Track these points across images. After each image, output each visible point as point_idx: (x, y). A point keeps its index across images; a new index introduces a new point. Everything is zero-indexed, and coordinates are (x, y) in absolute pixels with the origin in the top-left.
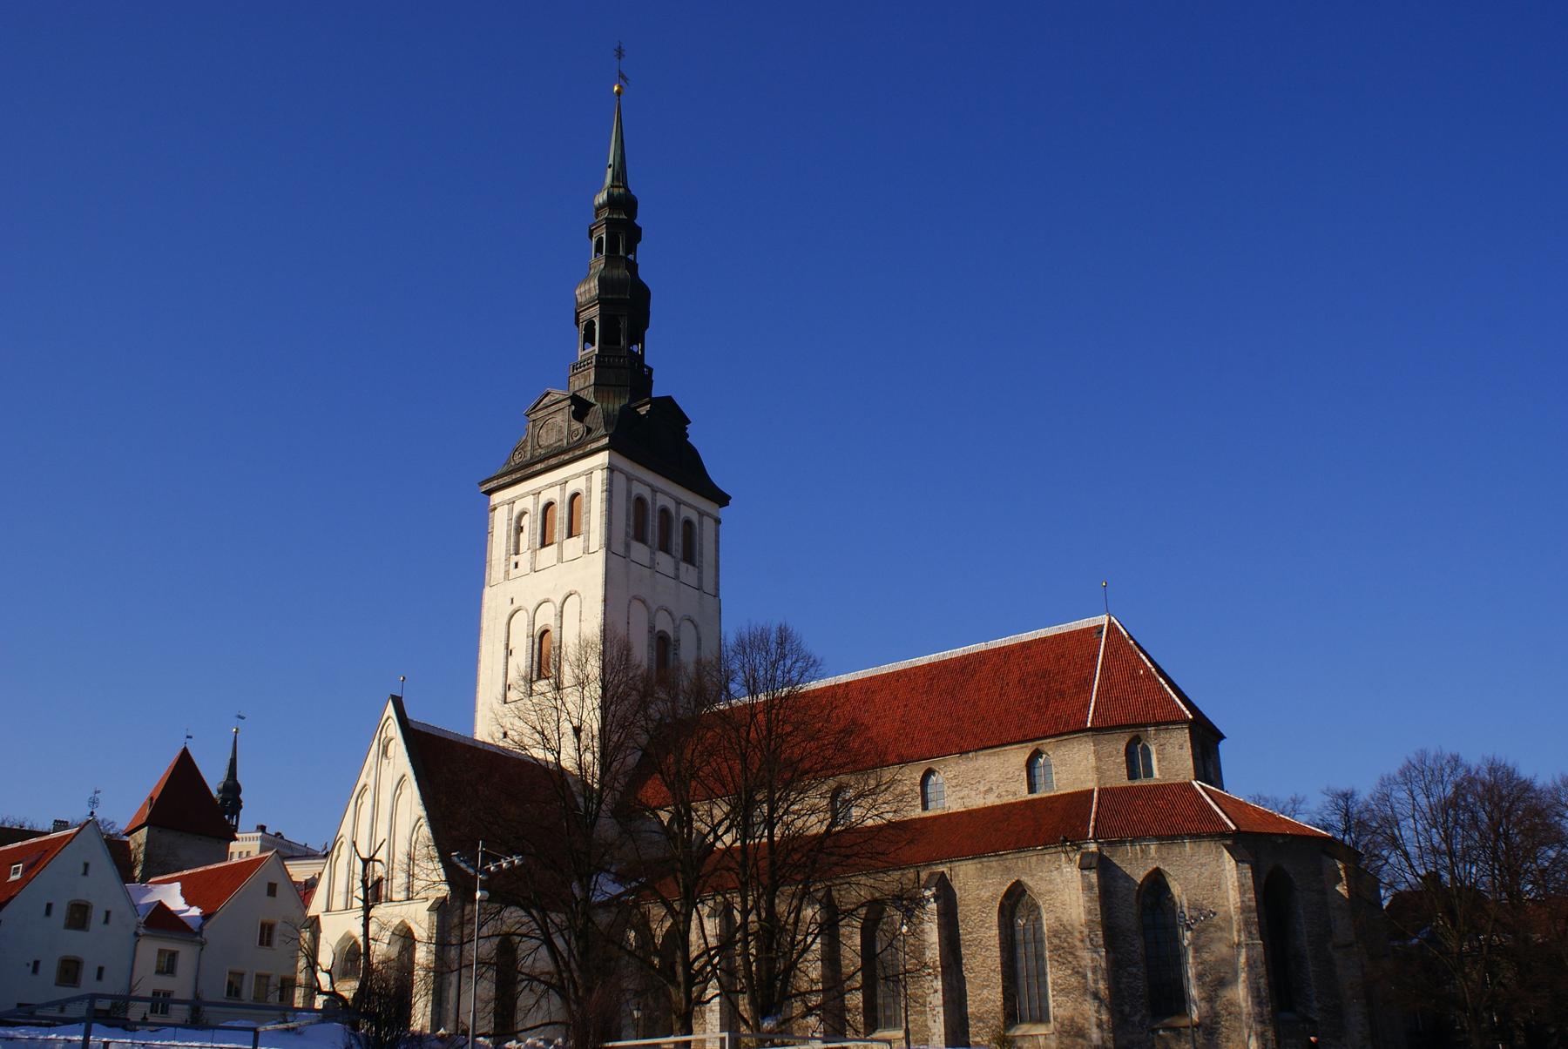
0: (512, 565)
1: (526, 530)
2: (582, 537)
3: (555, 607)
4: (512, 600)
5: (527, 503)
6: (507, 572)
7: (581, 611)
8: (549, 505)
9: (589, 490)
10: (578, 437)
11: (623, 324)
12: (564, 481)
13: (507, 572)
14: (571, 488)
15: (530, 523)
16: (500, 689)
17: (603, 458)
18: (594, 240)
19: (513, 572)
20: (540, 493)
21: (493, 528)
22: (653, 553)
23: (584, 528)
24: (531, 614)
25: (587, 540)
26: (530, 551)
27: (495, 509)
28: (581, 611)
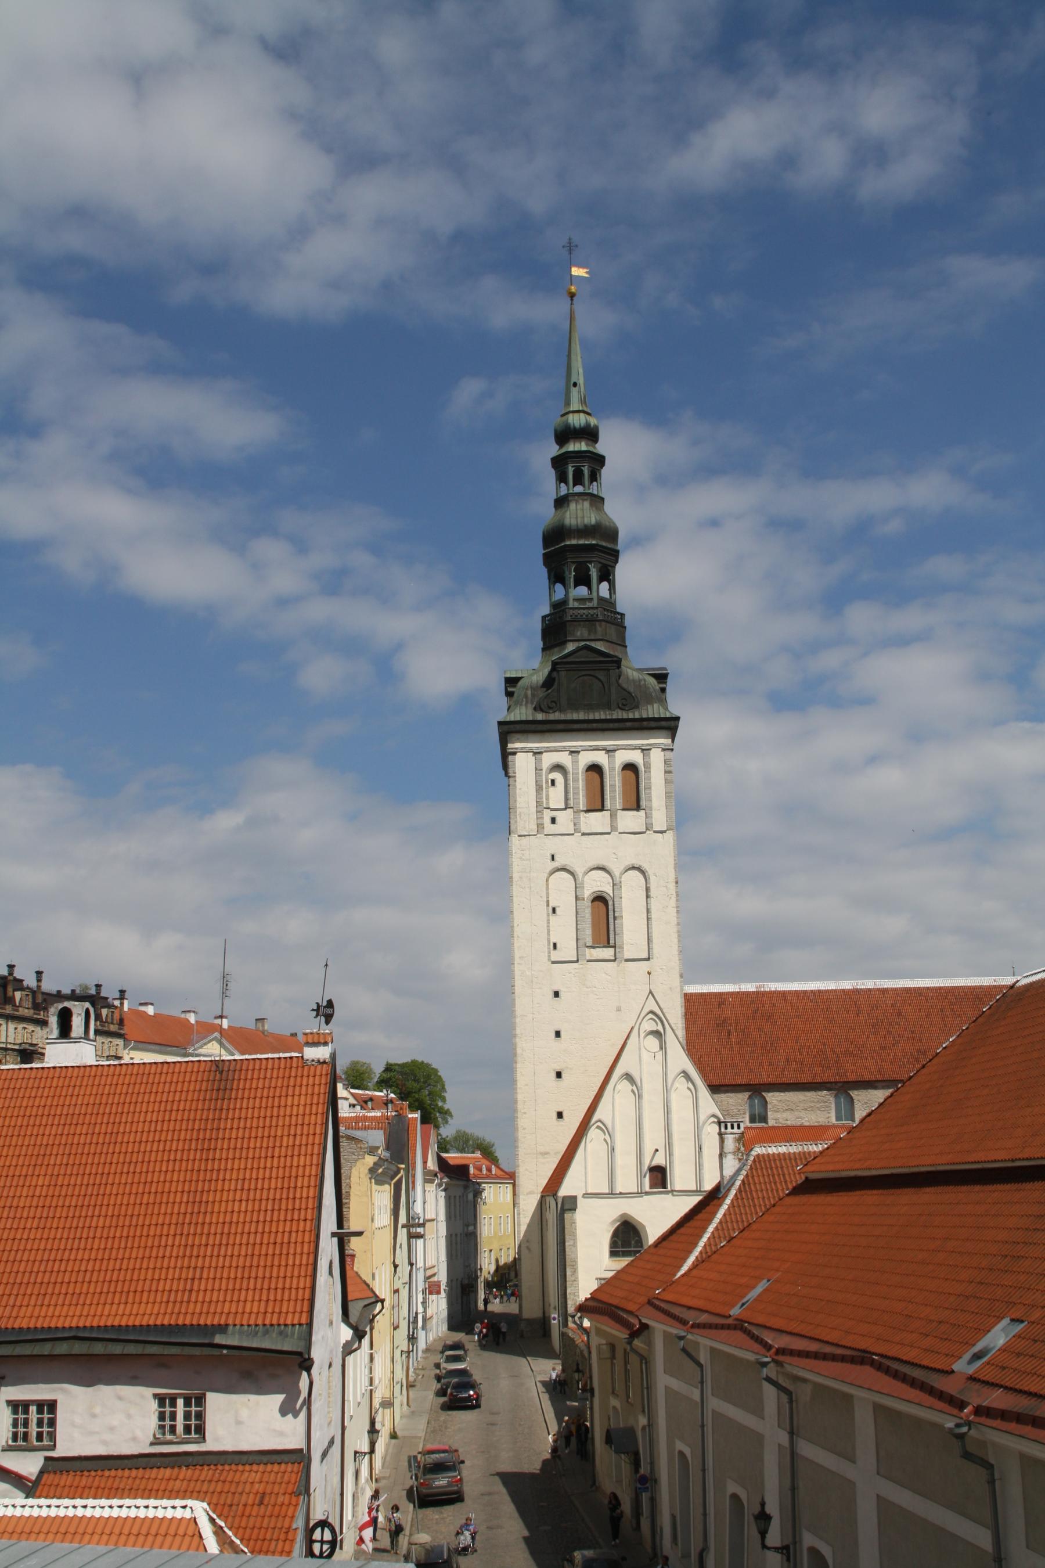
0: (547, 820)
2: (642, 813)
4: (553, 856)
5: (565, 759)
6: (540, 827)
9: (647, 766)
13: (540, 827)
14: (623, 757)
16: (542, 945)
19: (549, 827)
20: (578, 752)
23: (643, 803)
27: (514, 754)
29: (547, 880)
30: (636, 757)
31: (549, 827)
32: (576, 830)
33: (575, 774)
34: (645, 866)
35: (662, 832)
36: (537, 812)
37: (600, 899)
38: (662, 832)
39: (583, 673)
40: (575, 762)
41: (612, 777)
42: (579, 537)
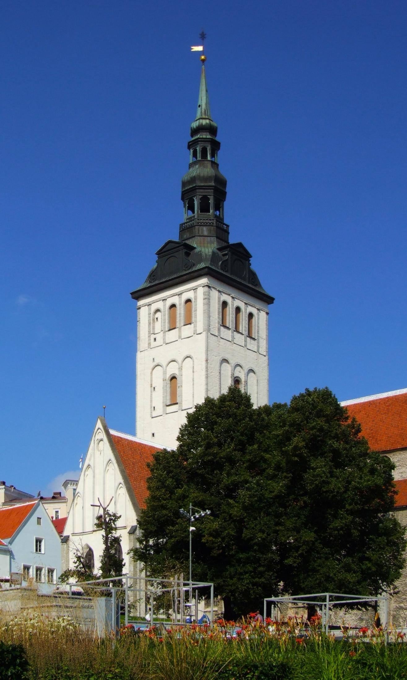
0: (152, 340)
1: (159, 319)
2: (193, 324)
3: (178, 364)
5: (160, 305)
6: (149, 344)
7: (193, 366)
8: (173, 306)
9: (196, 298)
10: (189, 267)
11: (211, 201)
12: (181, 292)
13: (149, 344)
14: (185, 297)
15: (162, 316)
17: (204, 281)
18: (192, 151)
19: (153, 344)
20: (166, 299)
21: (140, 319)
22: (232, 333)
23: (193, 320)
24: (164, 366)
25: (195, 327)
26: (162, 332)
27: (139, 308)
28: (193, 366)
29: (151, 373)
30: (190, 295)
31: (153, 344)
32: (164, 343)
33: (165, 312)
34: (192, 355)
35: (200, 334)
36: (149, 337)
37: (173, 378)
38: (200, 334)
39: (170, 256)
40: (165, 305)
41: (180, 309)
42: (189, 185)
